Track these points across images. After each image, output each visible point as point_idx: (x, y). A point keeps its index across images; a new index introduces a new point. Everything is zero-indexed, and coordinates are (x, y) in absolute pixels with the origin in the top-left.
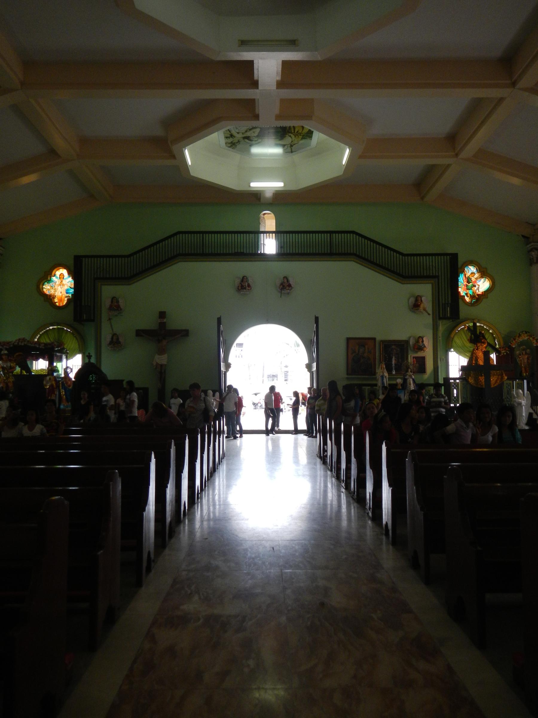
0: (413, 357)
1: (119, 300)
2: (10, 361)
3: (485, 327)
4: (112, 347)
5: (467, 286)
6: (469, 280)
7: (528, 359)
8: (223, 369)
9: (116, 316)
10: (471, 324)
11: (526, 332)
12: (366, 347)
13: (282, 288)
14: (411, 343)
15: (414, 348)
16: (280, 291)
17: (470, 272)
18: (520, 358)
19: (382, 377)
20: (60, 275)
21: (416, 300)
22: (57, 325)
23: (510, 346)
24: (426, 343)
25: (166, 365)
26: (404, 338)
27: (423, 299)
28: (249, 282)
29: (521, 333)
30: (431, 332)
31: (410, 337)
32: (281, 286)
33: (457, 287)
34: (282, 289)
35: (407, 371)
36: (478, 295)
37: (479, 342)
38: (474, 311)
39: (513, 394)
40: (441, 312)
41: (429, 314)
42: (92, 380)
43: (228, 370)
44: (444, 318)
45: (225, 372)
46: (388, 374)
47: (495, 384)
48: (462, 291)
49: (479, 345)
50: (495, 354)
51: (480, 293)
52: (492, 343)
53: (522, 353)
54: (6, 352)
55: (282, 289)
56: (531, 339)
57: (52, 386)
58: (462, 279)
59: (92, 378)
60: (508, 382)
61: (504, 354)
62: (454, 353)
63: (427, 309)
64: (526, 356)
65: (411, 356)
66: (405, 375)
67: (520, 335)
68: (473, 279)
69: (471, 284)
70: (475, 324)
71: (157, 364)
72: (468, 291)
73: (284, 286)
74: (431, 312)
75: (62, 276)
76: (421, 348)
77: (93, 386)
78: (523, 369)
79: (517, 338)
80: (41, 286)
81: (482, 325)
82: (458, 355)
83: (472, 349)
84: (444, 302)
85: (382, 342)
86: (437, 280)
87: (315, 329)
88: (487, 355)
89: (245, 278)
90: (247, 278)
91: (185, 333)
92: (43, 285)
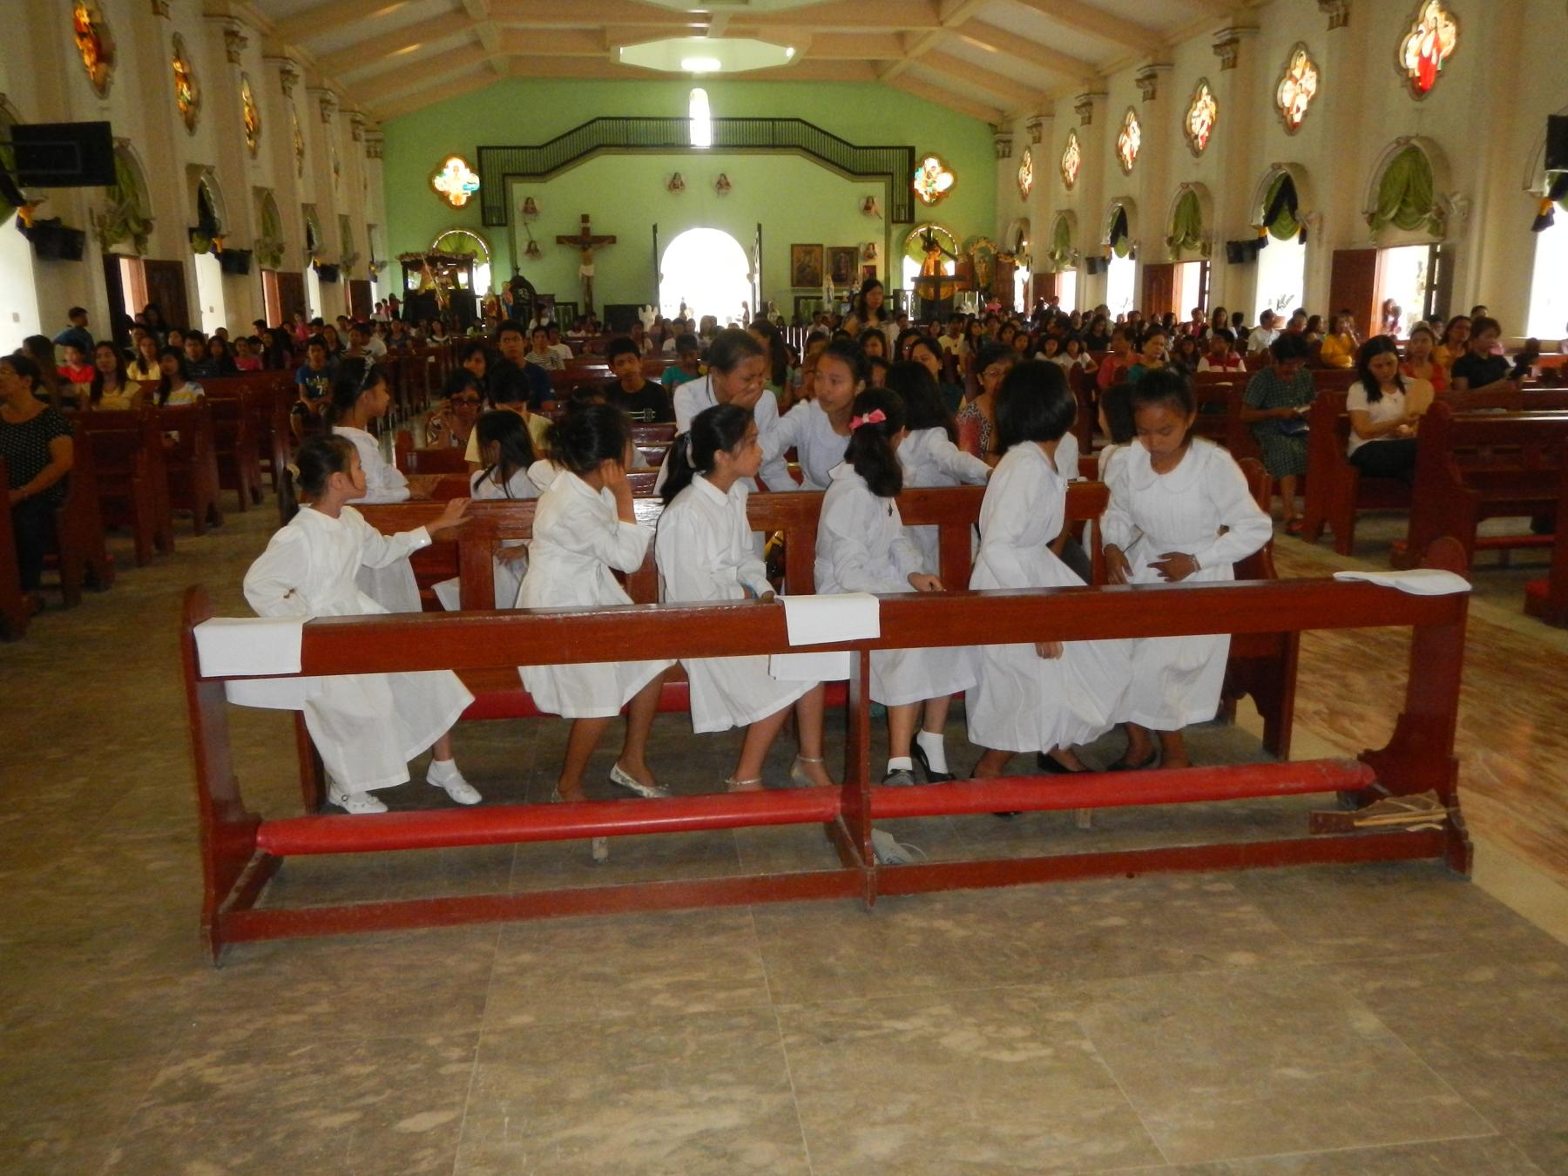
0: (864, 266)
19: (828, 290)
21: (868, 202)
24: (877, 250)
26: (851, 243)
30: (883, 237)
34: (719, 189)
38: (933, 213)
55: (719, 189)
57: (492, 302)
58: (920, 176)
66: (851, 287)
68: (934, 174)
70: (929, 231)
75: (456, 169)
76: (871, 256)
88: (938, 264)
91: (612, 240)
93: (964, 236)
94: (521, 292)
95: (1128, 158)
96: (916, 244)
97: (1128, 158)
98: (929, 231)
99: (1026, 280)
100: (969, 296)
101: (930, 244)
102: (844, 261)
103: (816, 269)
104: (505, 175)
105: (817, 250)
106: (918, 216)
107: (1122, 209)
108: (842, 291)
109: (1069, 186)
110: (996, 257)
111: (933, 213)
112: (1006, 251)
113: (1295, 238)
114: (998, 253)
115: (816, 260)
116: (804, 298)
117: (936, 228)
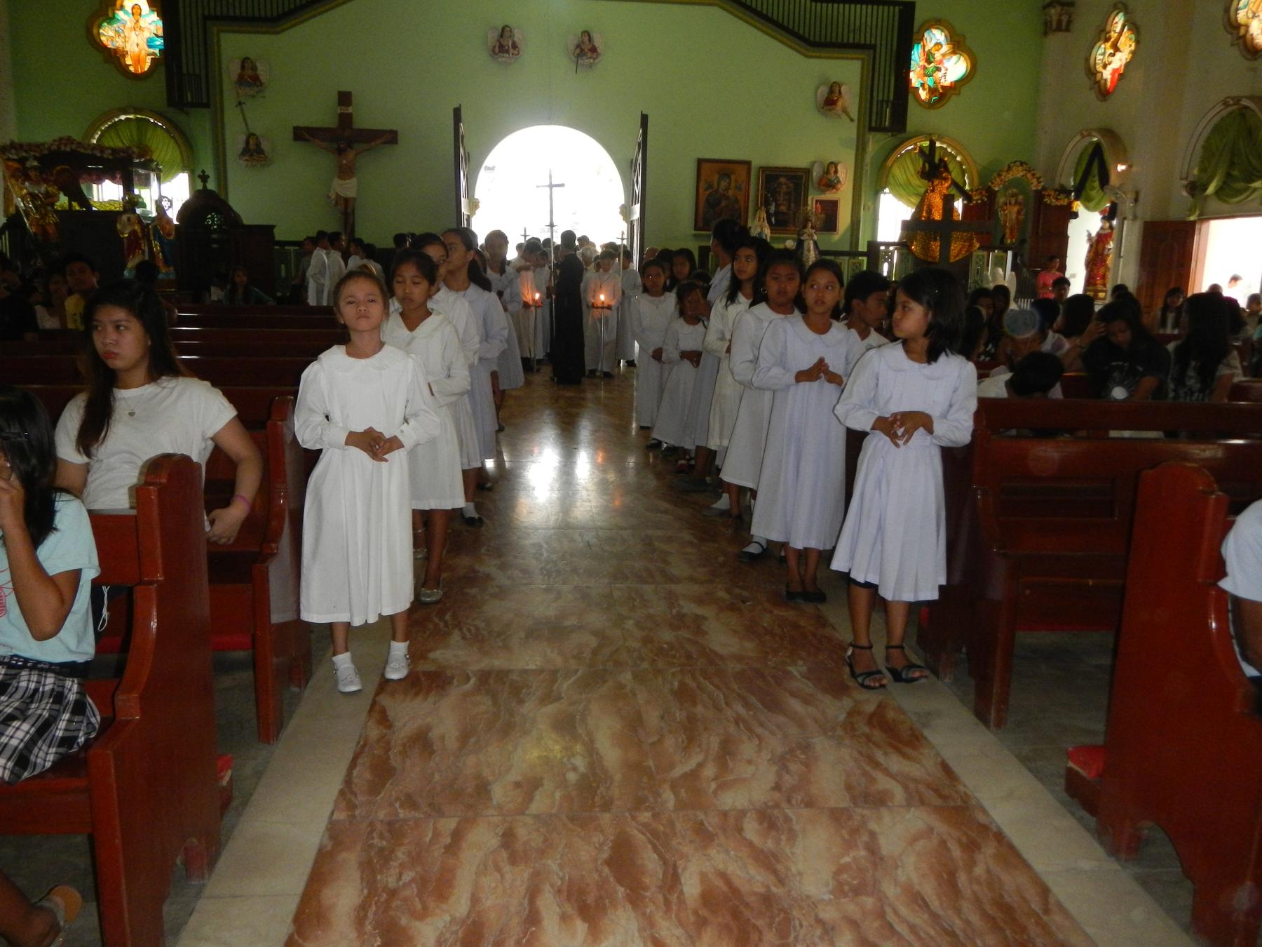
0: (817, 201)
1: (258, 65)
2: (46, 181)
3: (949, 150)
4: (247, 160)
5: (925, 68)
6: (929, 58)
7: (1019, 213)
8: (465, 210)
9: (253, 96)
10: (926, 144)
11: (1022, 164)
12: (733, 177)
13: (578, 55)
14: (814, 174)
15: (819, 184)
16: (575, 59)
17: (934, 42)
18: (1004, 210)
20: (133, 8)
21: (831, 91)
22: (135, 113)
23: (990, 187)
24: (841, 175)
25: (354, 199)
27: (843, 89)
28: (516, 39)
29: (1012, 165)
31: (813, 163)
32: (578, 51)
33: (908, 70)
35: (805, 227)
36: (943, 87)
37: (937, 178)
38: (935, 119)
39: (987, 276)
40: (874, 117)
41: (852, 120)
42: (211, 225)
43: (475, 213)
45: (468, 216)
46: (771, 230)
47: (957, 256)
48: (915, 79)
49: (936, 182)
50: (963, 200)
52: (959, 180)
53: (1010, 203)
54: (35, 163)
56: (1029, 175)
57: (134, 233)
58: (917, 55)
59: (212, 220)
60: (981, 253)
61: (977, 203)
62: (891, 195)
63: (849, 110)
64: (1016, 209)
65: (813, 199)
66: (800, 235)
67: (1009, 169)
68: (938, 56)
69: (932, 65)
70: (932, 144)
71: (338, 196)
72: (926, 78)
73: (582, 50)
74: (854, 115)
77: (215, 236)
78: (1008, 231)
79: (1004, 173)
80: (95, 31)
81: (945, 146)
83: (922, 190)
84: (880, 98)
85: (764, 169)
86: (872, 52)
87: (640, 139)
88: (948, 201)
89: (508, 29)
90: (511, 31)
91: (390, 137)
92: (100, 26)
96: (906, 167)
99: (1094, 234)
100: (996, 257)
101: (933, 168)
103: (737, 201)
104: (206, 18)
105: (742, 171)
108: (784, 240)
110: (1039, 195)
111: (935, 119)
112: (1057, 186)
114: (1044, 188)
115: (738, 188)
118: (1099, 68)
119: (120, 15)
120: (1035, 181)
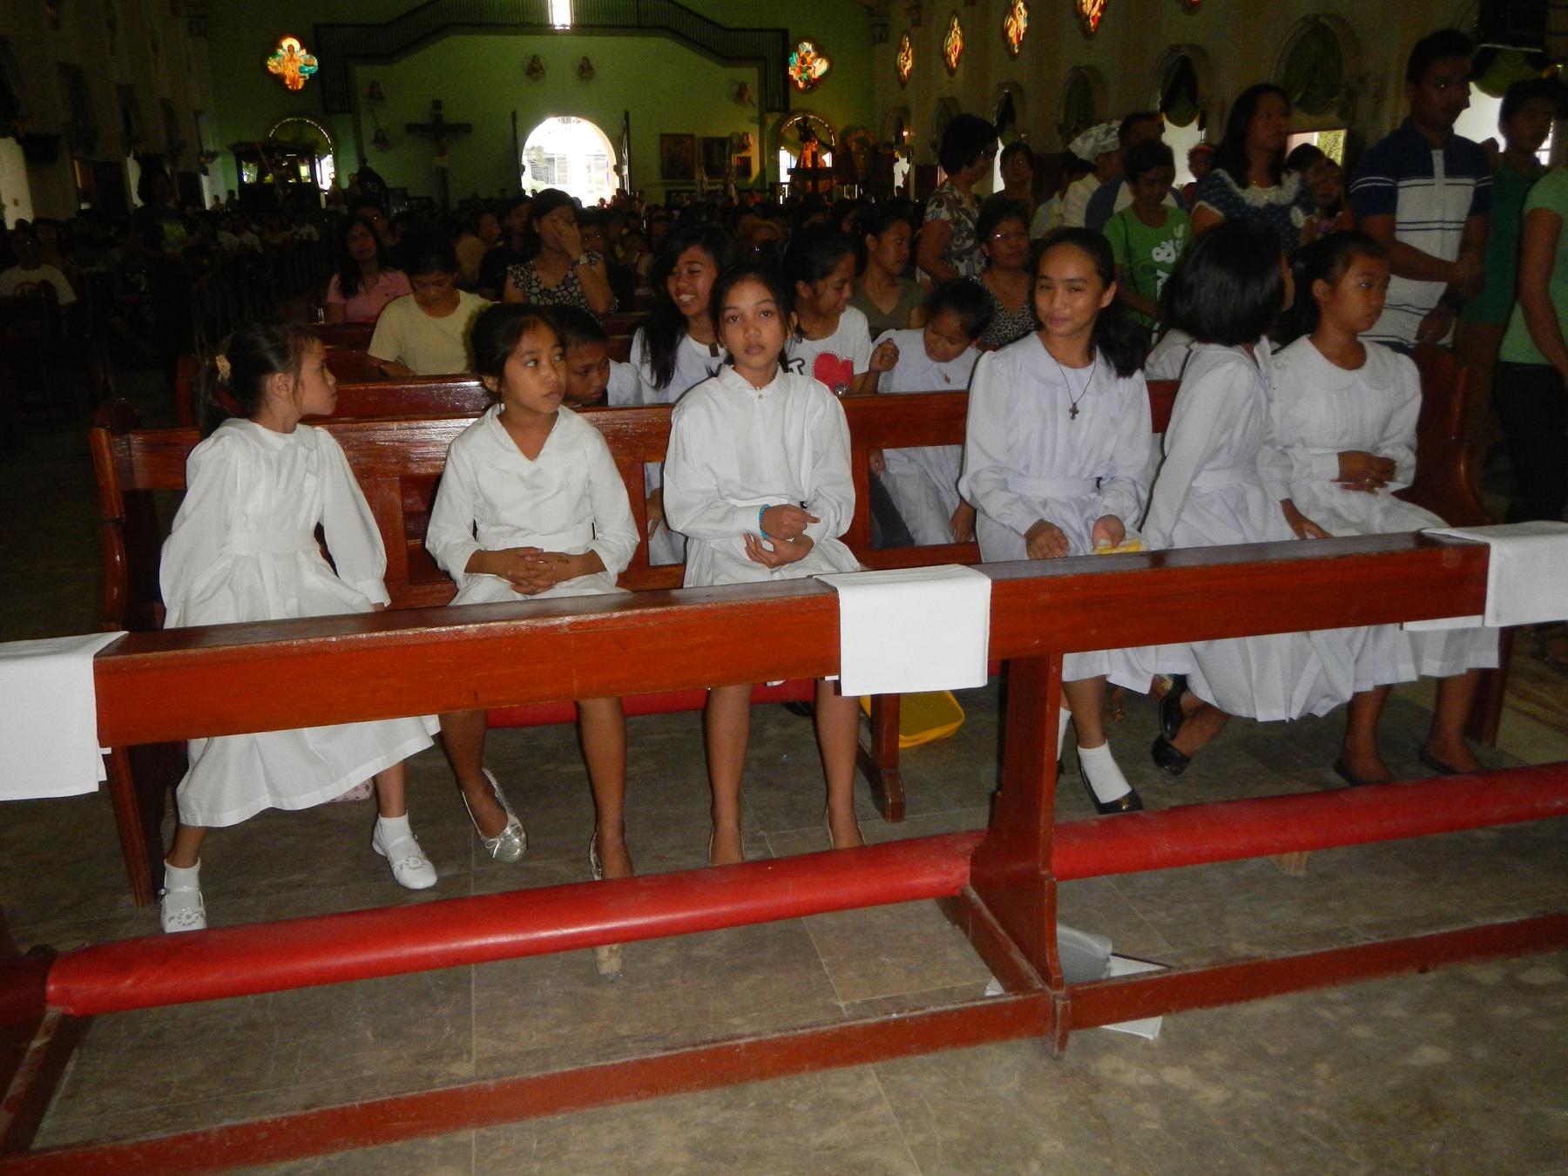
5: (801, 68)
6: (803, 60)
11: (863, 128)
21: (740, 88)
22: (297, 117)
24: (751, 140)
26: (724, 133)
27: (748, 86)
36: (814, 79)
44: (771, 110)
48: (793, 73)
51: (816, 77)
58: (795, 59)
60: (837, 187)
68: (808, 59)
70: (805, 120)
76: (744, 147)
82: (789, 154)
85: (703, 139)
88: (815, 156)
91: (465, 128)
92: (267, 59)
93: (840, 128)
94: (369, 185)
95: (1015, 41)
97: (1015, 41)
98: (805, 120)
99: (906, 172)
102: (717, 152)
106: (793, 107)
107: (1009, 96)
109: (952, 72)
113: (1194, 125)
114: (877, 144)
116: (675, 191)
117: (812, 117)
118: (902, 67)
119: (280, 52)
120: (871, 139)
